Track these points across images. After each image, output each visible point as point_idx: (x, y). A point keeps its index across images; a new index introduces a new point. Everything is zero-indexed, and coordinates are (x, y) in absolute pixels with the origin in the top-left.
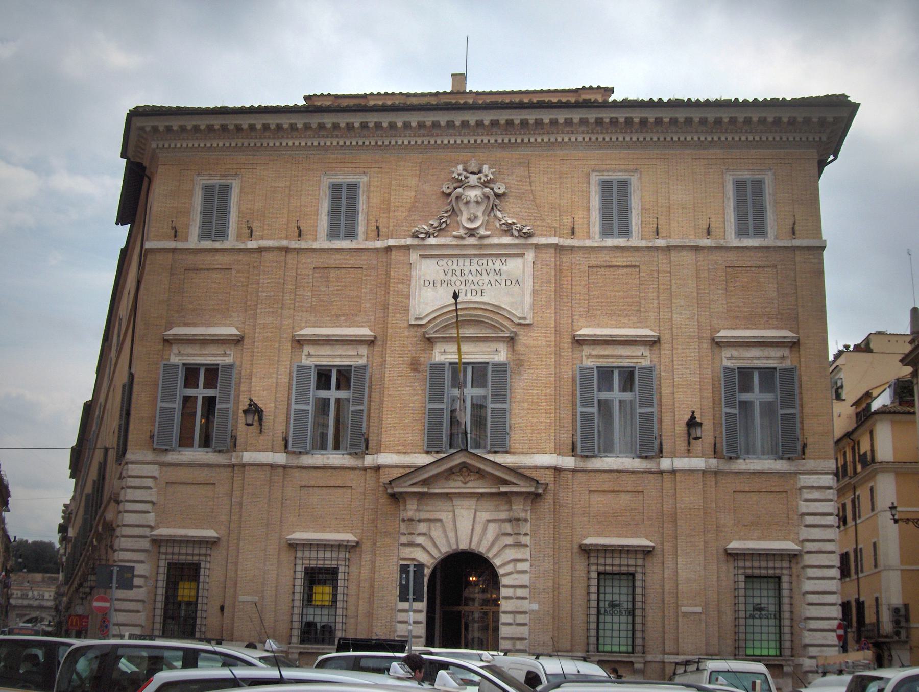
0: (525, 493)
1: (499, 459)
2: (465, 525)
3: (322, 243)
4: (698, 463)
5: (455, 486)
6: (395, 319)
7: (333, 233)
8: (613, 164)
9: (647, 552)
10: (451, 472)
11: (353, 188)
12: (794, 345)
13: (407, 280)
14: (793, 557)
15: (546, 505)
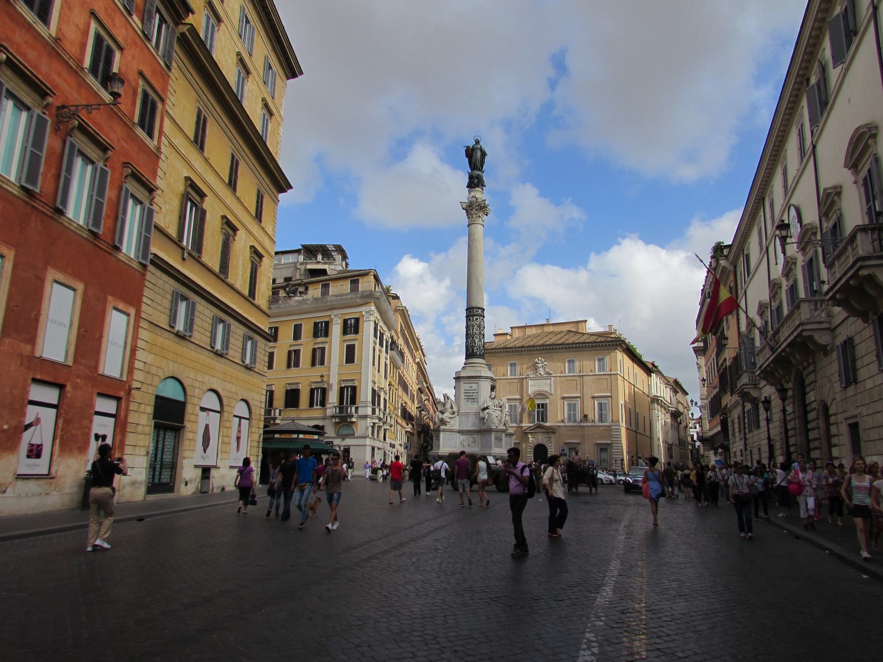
0: (551, 431)
1: (547, 424)
2: (541, 439)
3: (509, 377)
4: (589, 424)
5: (538, 430)
6: (525, 394)
7: (511, 375)
8: (571, 355)
9: (579, 444)
10: (536, 428)
11: (515, 364)
12: (611, 397)
13: (527, 385)
14: (610, 444)
15: (557, 433)
